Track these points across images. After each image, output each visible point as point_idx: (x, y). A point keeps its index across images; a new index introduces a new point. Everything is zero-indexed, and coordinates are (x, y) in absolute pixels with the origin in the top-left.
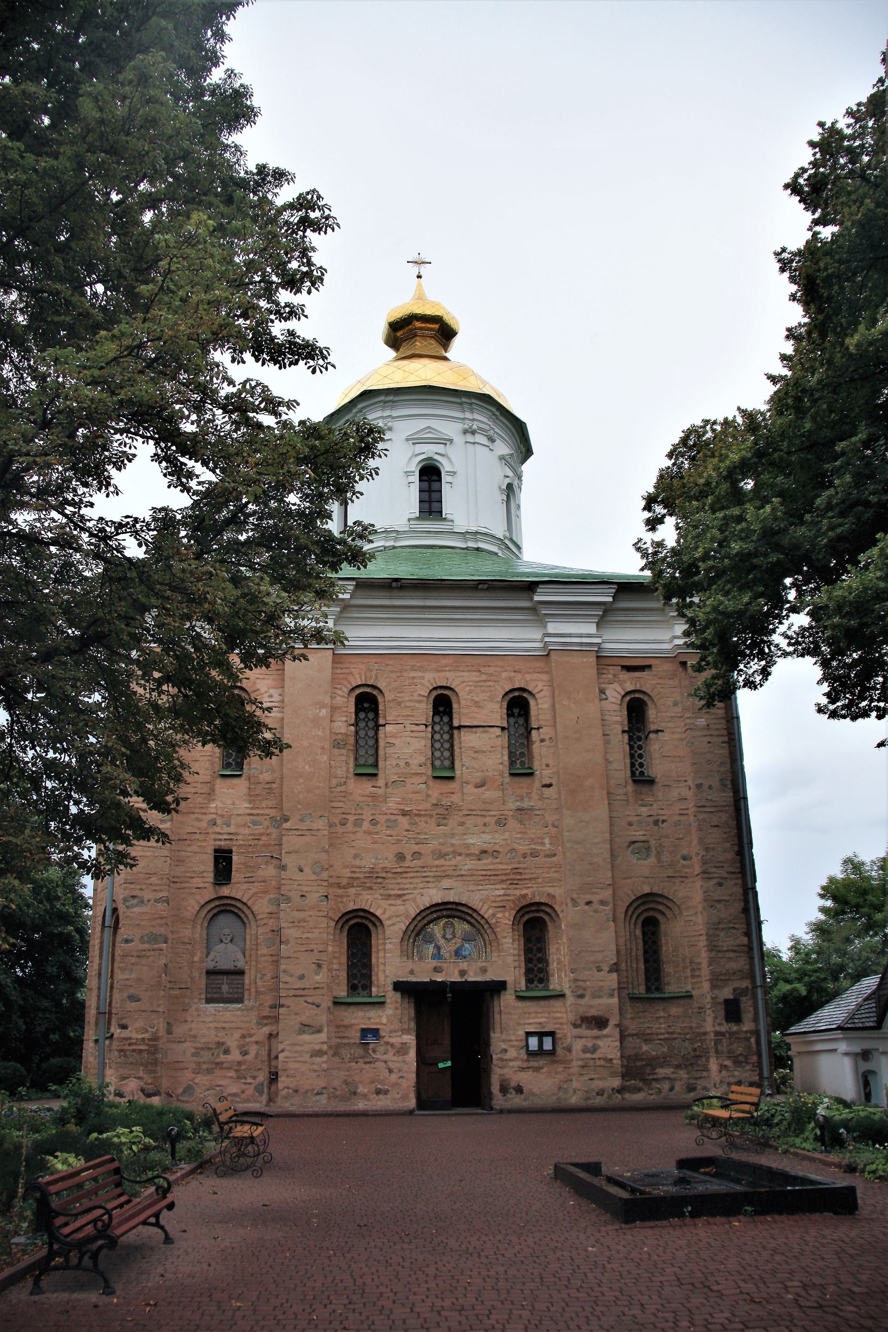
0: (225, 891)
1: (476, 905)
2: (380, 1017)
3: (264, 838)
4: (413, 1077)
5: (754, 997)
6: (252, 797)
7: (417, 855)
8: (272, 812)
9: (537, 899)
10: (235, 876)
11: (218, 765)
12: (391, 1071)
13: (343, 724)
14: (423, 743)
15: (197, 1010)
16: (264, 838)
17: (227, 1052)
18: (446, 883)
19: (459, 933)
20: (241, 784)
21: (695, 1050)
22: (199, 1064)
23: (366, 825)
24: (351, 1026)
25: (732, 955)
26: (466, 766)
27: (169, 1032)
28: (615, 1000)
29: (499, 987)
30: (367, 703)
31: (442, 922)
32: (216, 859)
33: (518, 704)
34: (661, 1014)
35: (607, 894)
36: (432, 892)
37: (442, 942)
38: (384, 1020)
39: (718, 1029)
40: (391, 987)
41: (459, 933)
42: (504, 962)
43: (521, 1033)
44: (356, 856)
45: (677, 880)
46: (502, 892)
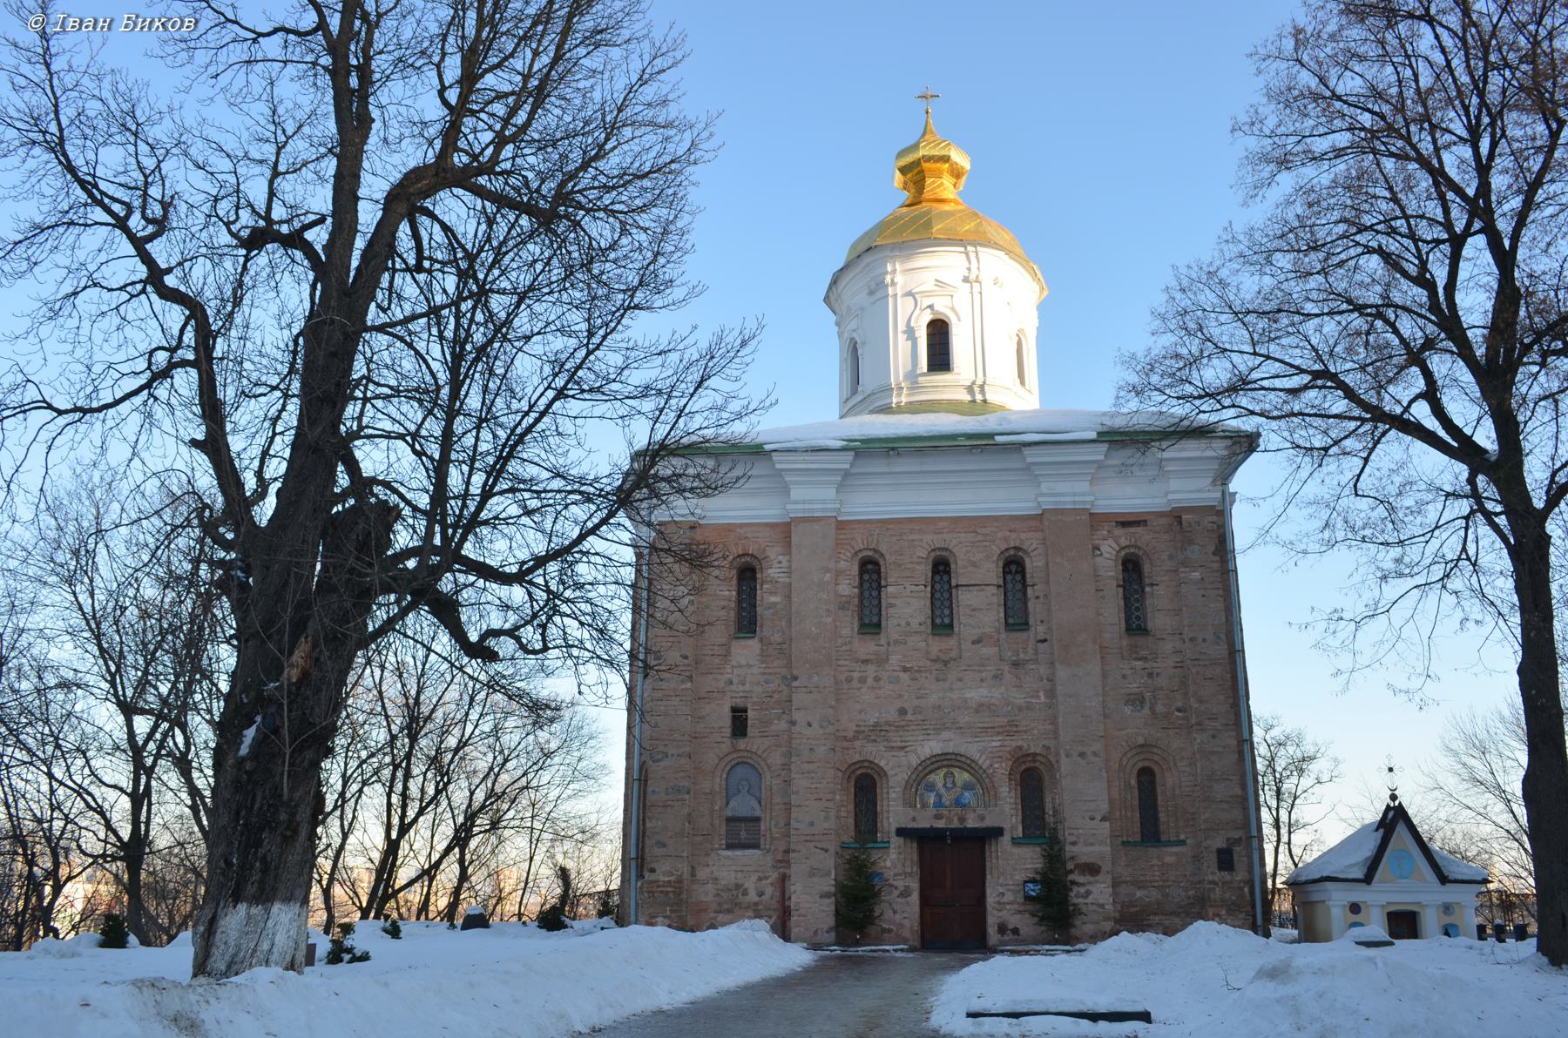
0: (742, 743)
4: (917, 916)
5: (1249, 845)
6: (764, 657)
7: (918, 710)
8: (784, 671)
11: (732, 631)
13: (848, 588)
17: (745, 893)
18: (946, 735)
19: (959, 783)
20: (753, 645)
22: (720, 904)
23: (870, 680)
25: (1225, 806)
26: (966, 626)
29: (998, 832)
30: (870, 570)
31: (942, 773)
32: (734, 718)
33: (1013, 566)
34: (1155, 862)
35: (1098, 746)
36: (933, 744)
37: (943, 791)
39: (1210, 878)
40: (893, 834)
41: (959, 783)
42: (1006, 812)
44: (860, 712)
45: (1171, 732)
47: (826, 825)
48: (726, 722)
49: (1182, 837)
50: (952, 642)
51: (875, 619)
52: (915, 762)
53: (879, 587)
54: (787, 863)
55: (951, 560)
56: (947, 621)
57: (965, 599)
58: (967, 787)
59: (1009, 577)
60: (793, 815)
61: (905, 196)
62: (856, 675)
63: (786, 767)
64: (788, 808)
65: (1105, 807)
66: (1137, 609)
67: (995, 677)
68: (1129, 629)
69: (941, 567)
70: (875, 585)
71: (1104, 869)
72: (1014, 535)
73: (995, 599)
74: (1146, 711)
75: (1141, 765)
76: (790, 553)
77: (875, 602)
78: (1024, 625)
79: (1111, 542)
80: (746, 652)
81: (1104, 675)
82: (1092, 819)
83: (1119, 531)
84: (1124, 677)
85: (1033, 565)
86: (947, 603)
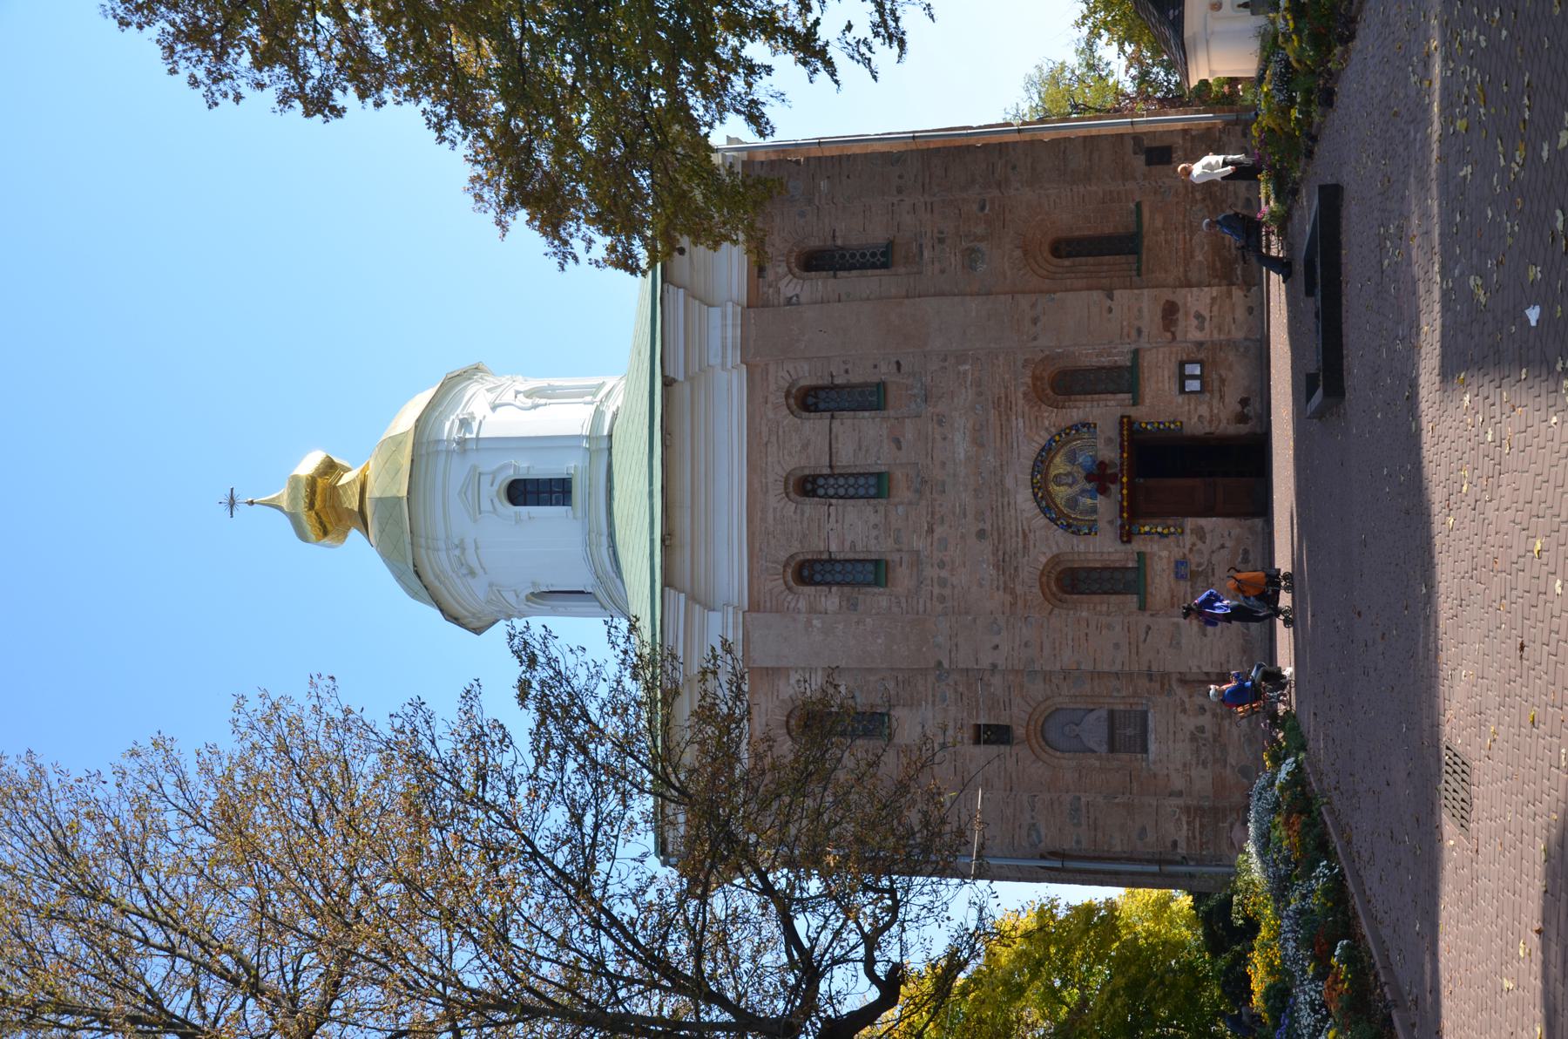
0: (1019, 732)
1: (1036, 447)
2: (1161, 558)
3: (960, 689)
7: (980, 516)
9: (1029, 381)
10: (1004, 720)
12: (1223, 546)
13: (831, 600)
14: (850, 508)
15: (1155, 763)
16: (960, 689)
17: (1201, 729)
18: (1009, 483)
21: (1204, 199)
23: (944, 573)
24: (1171, 590)
26: (879, 457)
27: (1180, 794)
28: (1146, 291)
29: (1127, 423)
30: (810, 572)
31: (1054, 488)
32: (986, 742)
33: (809, 400)
34: (1162, 238)
35: (1024, 302)
36: (1020, 498)
37: (1077, 488)
38: (1165, 554)
40: (1129, 546)
43: (1180, 399)
44: (981, 586)
46: (1020, 420)
47: (1118, 628)
48: (993, 750)
49: (1132, 205)
50: (899, 474)
51: (871, 567)
52: (1042, 521)
53: (831, 561)
54: (1165, 676)
55: (800, 473)
56: (872, 481)
57: (847, 457)
58: (1072, 457)
59: (822, 406)
60: (1106, 668)
61: (355, 535)
62: (936, 591)
63: (1047, 676)
64: (1097, 675)
65: (1096, 295)
66: (863, 255)
67: (940, 423)
68: (885, 266)
69: (807, 486)
70: (828, 567)
71: (1171, 297)
72: (772, 398)
73: (849, 422)
74: (983, 246)
75: (1047, 254)
76: (787, 669)
77: (849, 567)
78: (881, 387)
79: (782, 284)
80: (908, 726)
81: (942, 294)
82: (1110, 310)
83: (770, 275)
84: (943, 271)
85: (808, 376)
86: (852, 481)
